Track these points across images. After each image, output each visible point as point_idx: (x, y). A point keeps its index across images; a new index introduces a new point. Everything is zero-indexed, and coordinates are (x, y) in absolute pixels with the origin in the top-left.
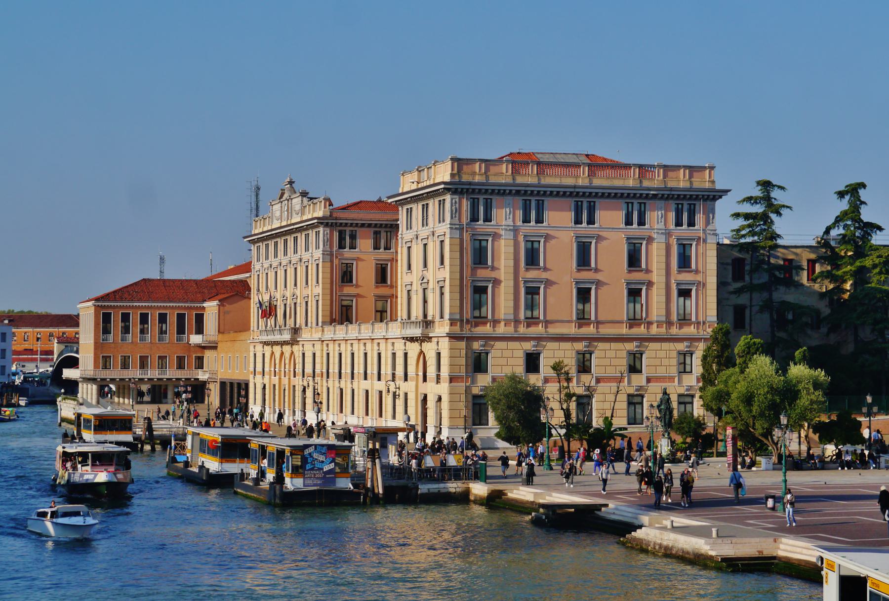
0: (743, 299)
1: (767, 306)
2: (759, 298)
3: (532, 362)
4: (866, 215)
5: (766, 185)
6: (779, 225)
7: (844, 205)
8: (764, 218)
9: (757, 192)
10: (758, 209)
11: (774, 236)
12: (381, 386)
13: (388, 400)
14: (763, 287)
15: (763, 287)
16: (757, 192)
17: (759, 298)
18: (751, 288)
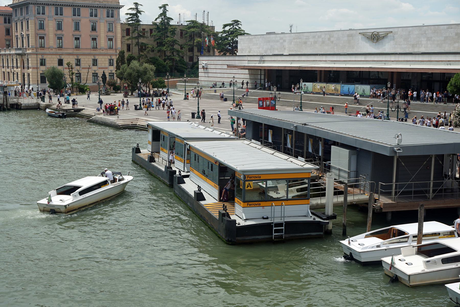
0: (130, 42)
1: (137, 44)
2: (135, 41)
3: (60, 62)
4: (168, 15)
5: (136, 4)
6: (141, 17)
7: (161, 11)
8: (136, 14)
9: (134, 6)
10: (134, 12)
11: (139, 21)
12: (8, 70)
13: (11, 75)
14: (136, 38)
15: (136, 38)
16: (134, 6)
17: (135, 41)
18: (132, 38)
